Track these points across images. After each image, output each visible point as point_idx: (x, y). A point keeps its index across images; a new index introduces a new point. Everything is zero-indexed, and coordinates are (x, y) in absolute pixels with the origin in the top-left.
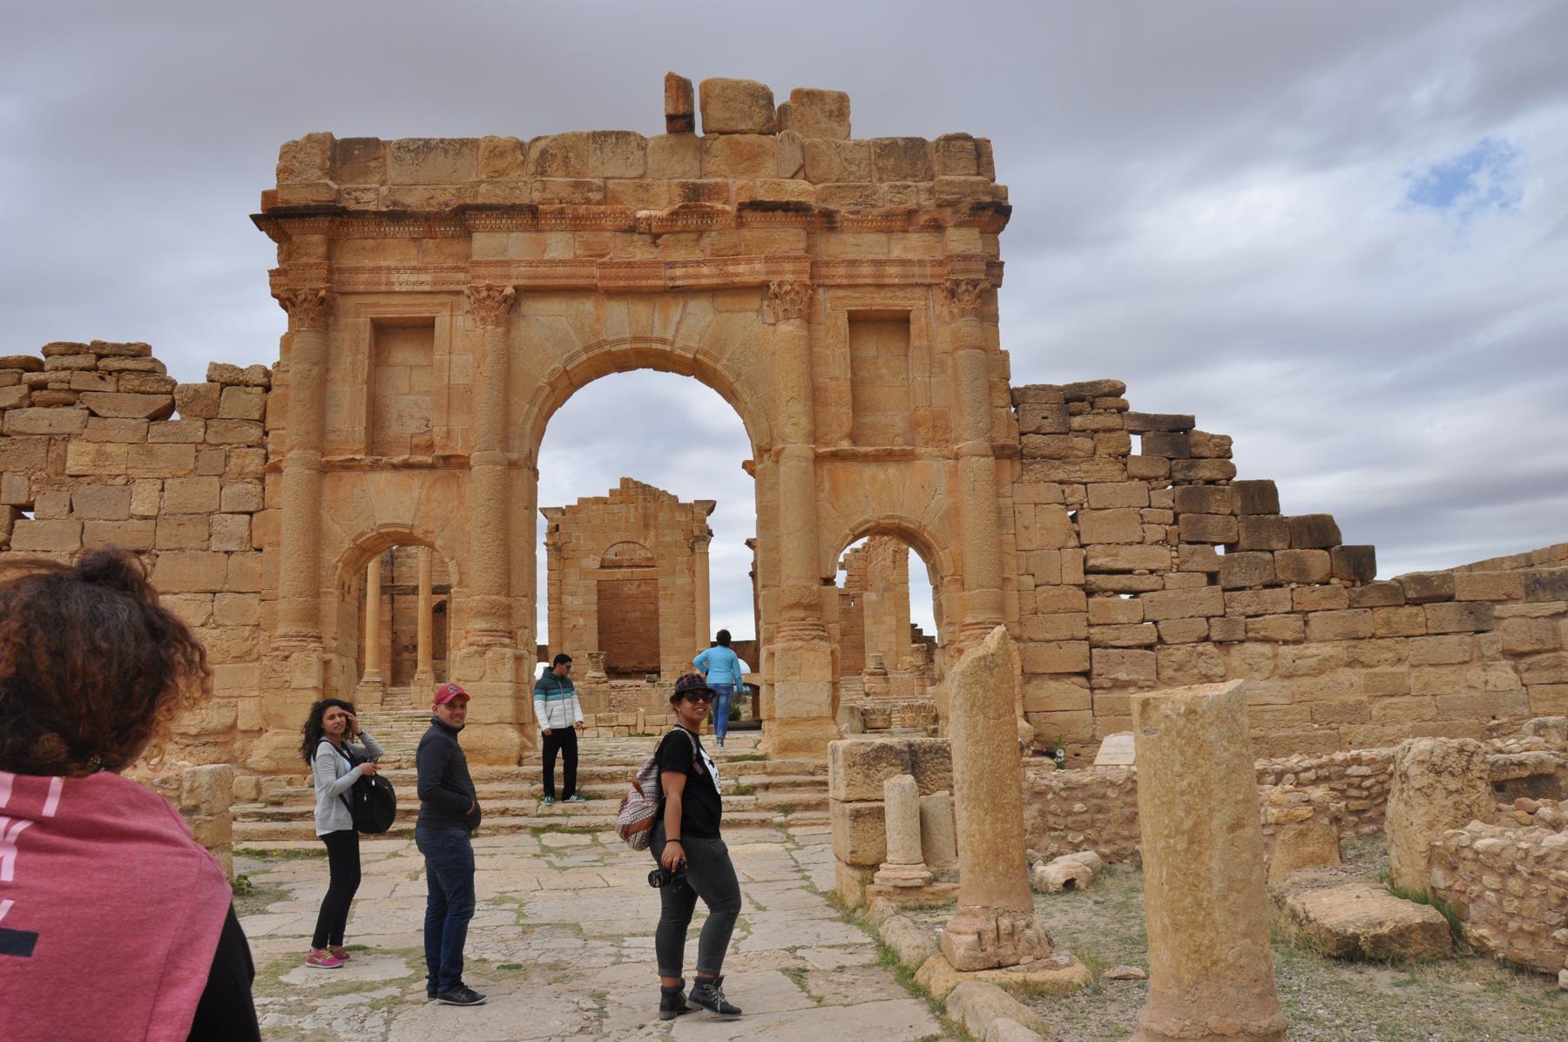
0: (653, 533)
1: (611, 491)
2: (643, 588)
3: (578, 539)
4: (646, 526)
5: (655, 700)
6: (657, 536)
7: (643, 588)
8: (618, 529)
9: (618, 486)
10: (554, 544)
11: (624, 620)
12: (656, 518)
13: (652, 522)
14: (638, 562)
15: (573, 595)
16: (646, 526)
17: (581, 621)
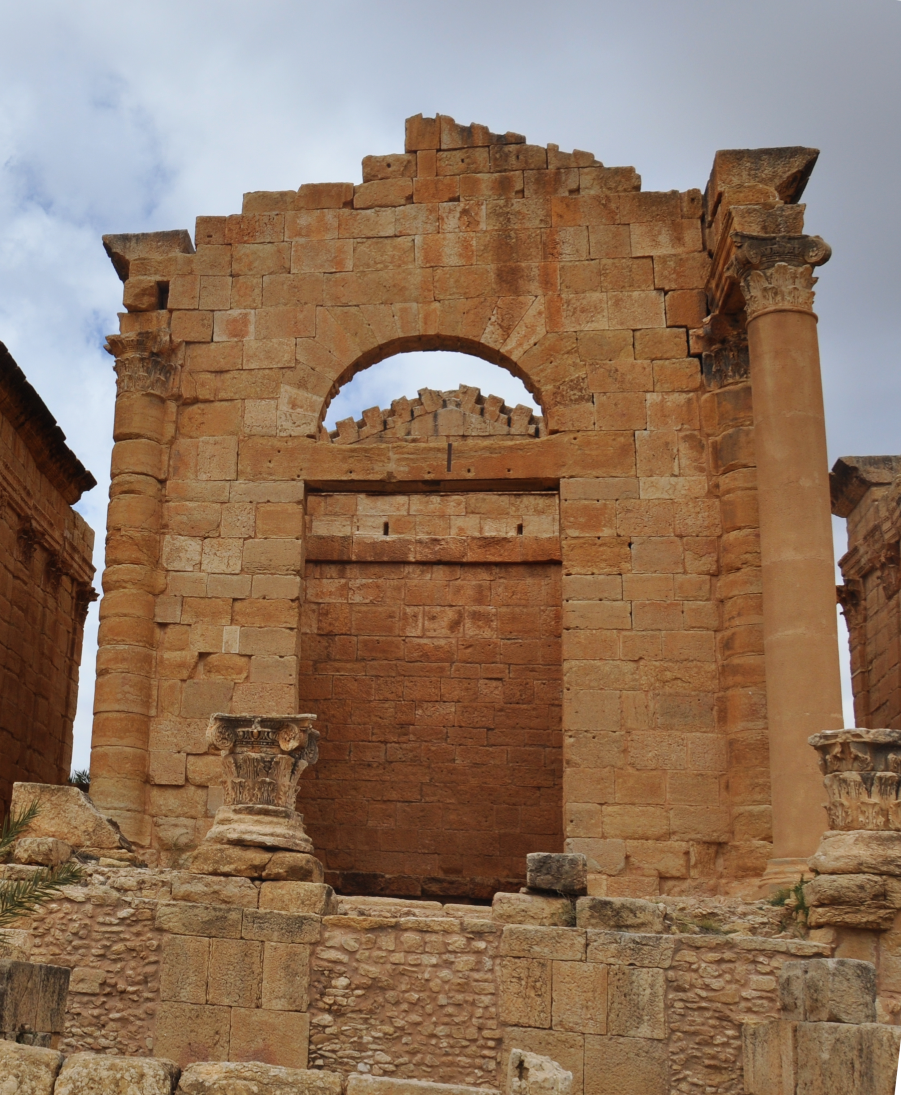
0: (534, 306)
1: (369, 163)
2: (469, 629)
3: (237, 330)
4: (510, 279)
5: (575, 999)
6: (553, 315)
7: (469, 629)
8: (398, 291)
9: (393, 144)
10: (142, 342)
11: (403, 727)
12: (550, 249)
13: (533, 265)
14: (454, 550)
15: (206, 533)
16: (510, 279)
17: (231, 638)
